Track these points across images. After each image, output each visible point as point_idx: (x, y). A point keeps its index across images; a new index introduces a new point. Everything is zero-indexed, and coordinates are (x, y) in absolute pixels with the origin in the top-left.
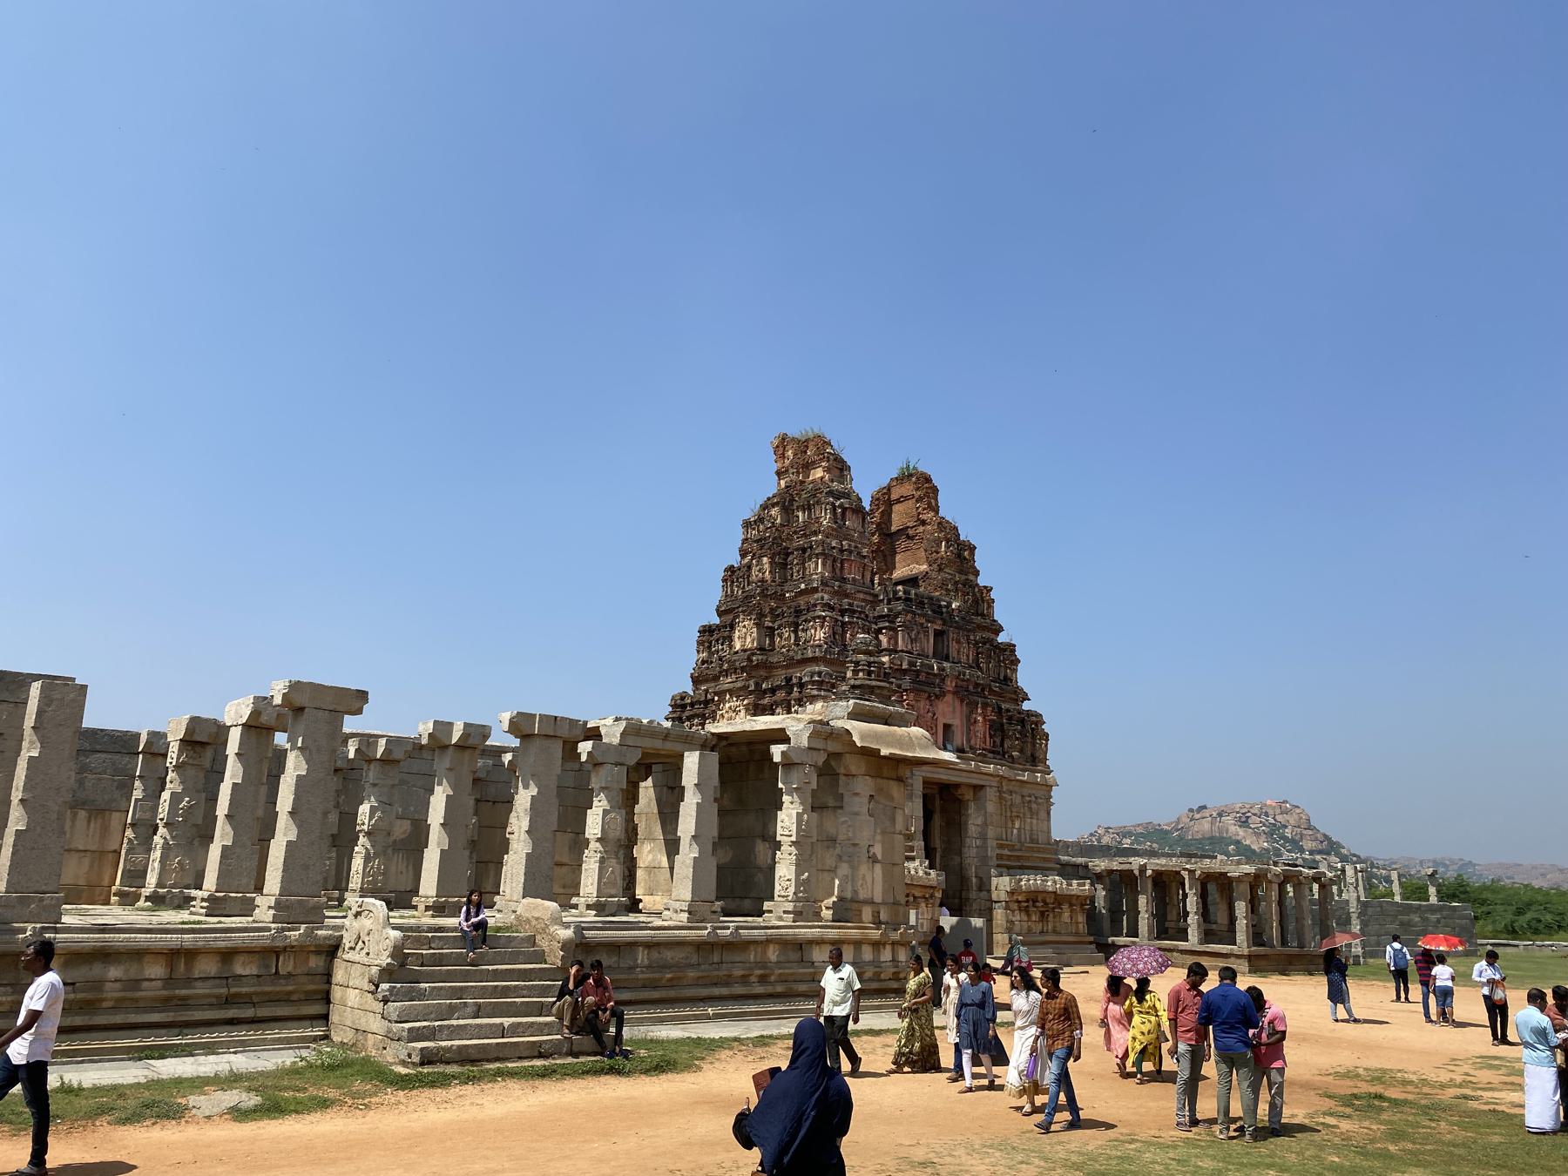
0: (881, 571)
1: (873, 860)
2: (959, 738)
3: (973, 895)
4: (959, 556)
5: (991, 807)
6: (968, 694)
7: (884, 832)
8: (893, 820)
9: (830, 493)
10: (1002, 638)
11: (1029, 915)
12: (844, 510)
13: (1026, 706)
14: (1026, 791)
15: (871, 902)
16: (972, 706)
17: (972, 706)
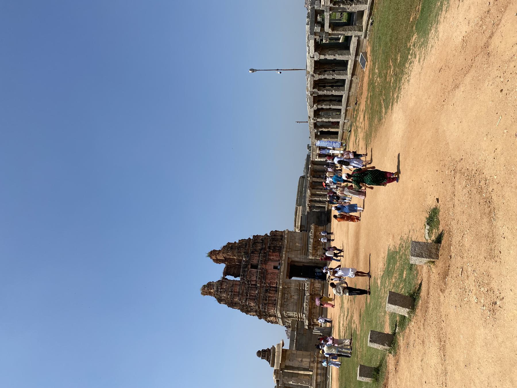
0: (234, 262)
1: (302, 361)
2: (277, 264)
3: (313, 261)
4: (231, 248)
5: (293, 256)
6: (266, 261)
7: (296, 357)
8: (294, 354)
9: (217, 291)
10: (252, 238)
11: (318, 249)
12: (221, 288)
13: (269, 234)
14: (289, 241)
15: (310, 362)
16: (269, 260)
17: (269, 260)
